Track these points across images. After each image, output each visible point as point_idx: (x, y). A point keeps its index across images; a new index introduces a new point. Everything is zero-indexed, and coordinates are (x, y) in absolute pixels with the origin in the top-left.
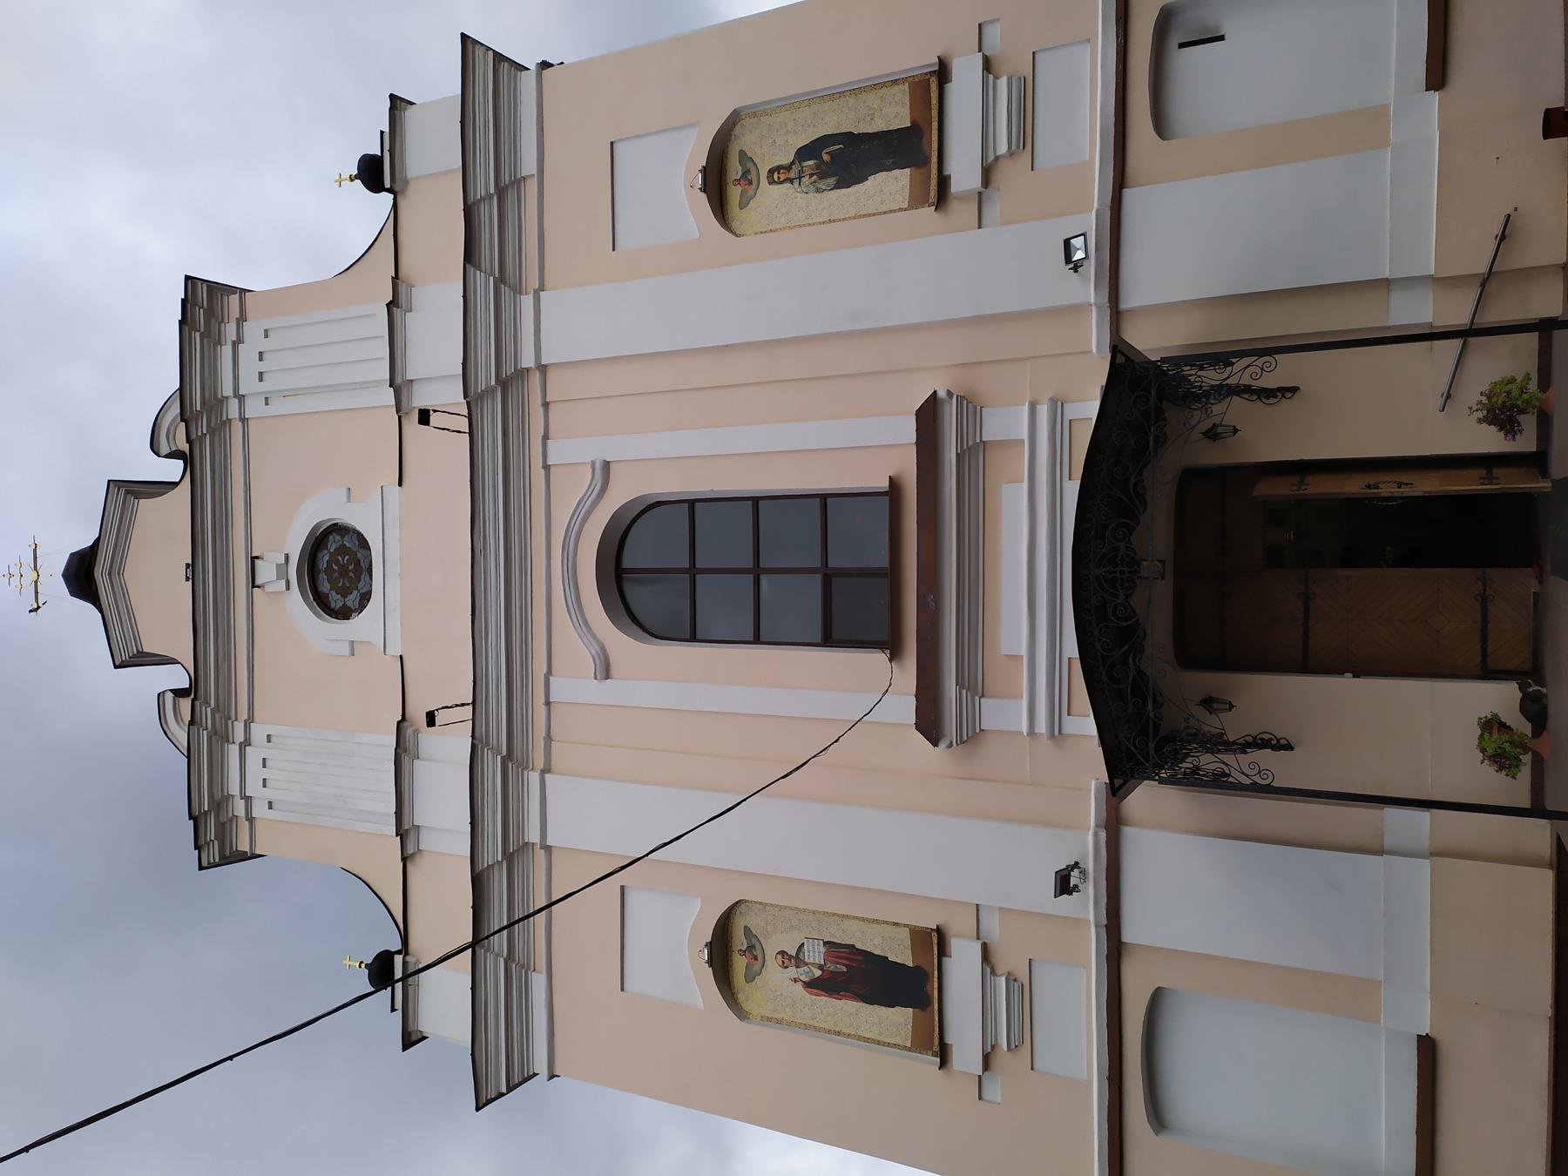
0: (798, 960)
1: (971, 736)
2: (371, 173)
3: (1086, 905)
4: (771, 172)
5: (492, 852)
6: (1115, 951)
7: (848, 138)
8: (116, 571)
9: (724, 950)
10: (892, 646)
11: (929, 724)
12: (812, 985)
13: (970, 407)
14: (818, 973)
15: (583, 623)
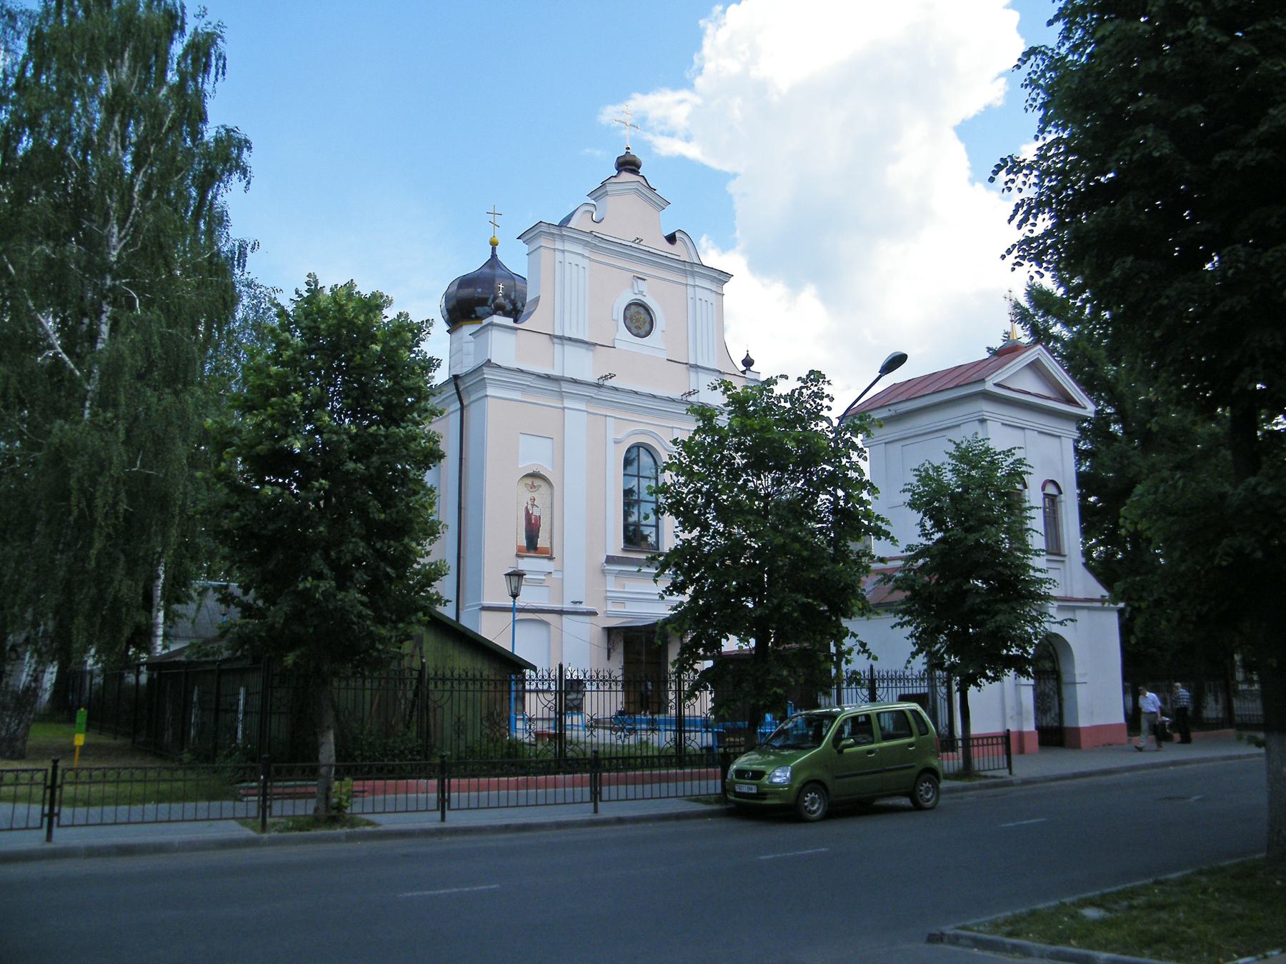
0: (533, 505)
3: (567, 606)
6: (561, 612)
10: (624, 550)
11: (610, 560)
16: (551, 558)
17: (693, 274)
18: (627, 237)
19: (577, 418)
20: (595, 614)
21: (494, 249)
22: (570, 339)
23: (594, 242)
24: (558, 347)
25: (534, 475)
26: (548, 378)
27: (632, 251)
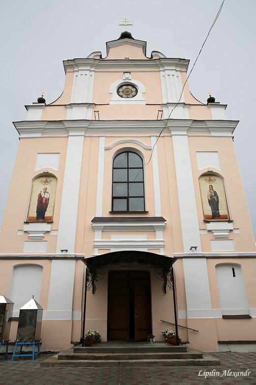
0: (45, 192)
1: (94, 229)
2: (211, 100)
3: (58, 253)
4: (212, 186)
5: (67, 125)
6: (50, 258)
7: (218, 202)
8: (127, 43)
9: (47, 176)
11: (96, 220)
12: (40, 196)
13: (164, 228)
14: (43, 196)
15: (116, 145)
22: (75, 104)
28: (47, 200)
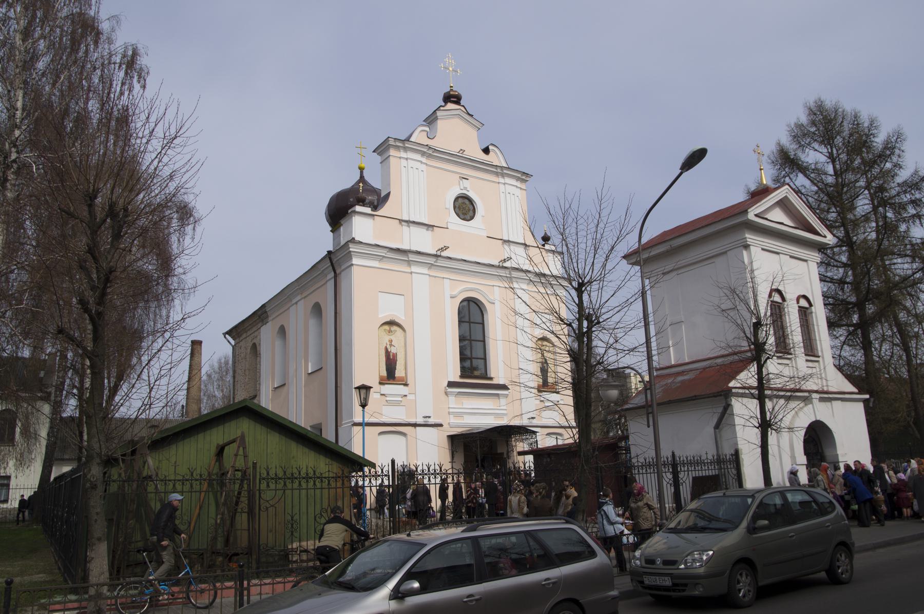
0: (391, 345)
3: (420, 420)
6: (415, 425)
10: (462, 376)
11: (451, 384)
16: (406, 385)
17: (503, 175)
18: (454, 149)
19: (421, 279)
20: (441, 425)
21: (362, 173)
22: (414, 222)
23: (430, 153)
24: (405, 228)
25: (391, 323)
26: (398, 250)
27: (458, 159)
28: (395, 355)
